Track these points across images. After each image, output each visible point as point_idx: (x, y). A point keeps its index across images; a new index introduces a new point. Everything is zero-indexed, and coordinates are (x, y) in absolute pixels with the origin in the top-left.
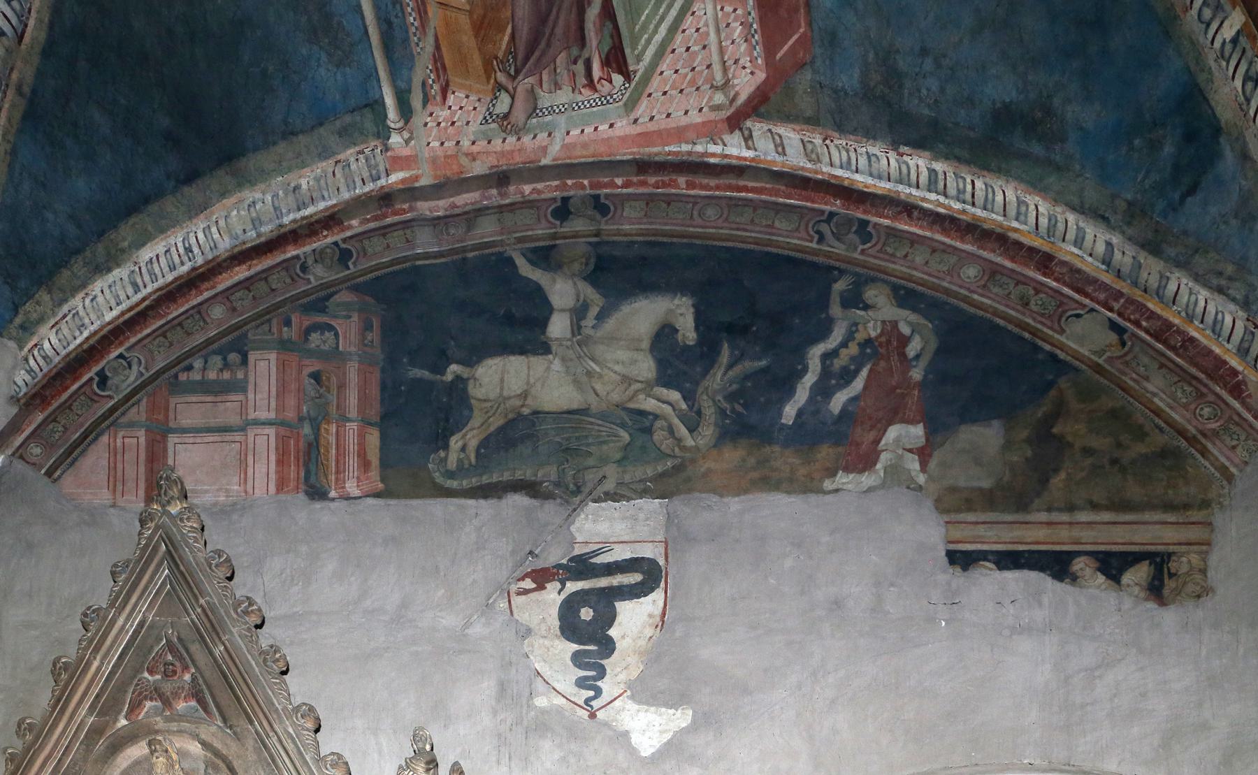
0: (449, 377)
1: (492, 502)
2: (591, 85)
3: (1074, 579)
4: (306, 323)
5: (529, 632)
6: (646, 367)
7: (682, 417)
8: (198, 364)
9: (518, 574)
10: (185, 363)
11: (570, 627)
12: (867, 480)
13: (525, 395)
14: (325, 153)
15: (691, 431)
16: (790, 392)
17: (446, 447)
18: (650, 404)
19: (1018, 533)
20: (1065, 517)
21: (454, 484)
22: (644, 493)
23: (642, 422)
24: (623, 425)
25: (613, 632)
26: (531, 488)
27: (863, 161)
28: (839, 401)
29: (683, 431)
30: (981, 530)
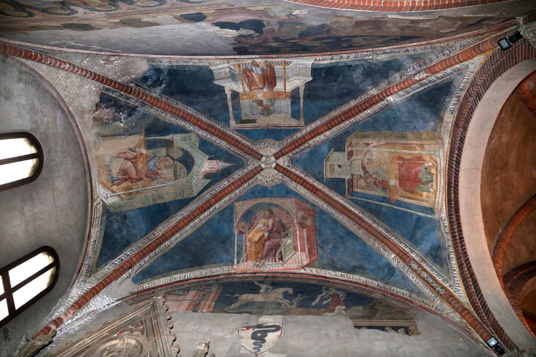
0: (235, 296)
1: (239, 315)
2: (275, 262)
3: (386, 331)
4: (205, 287)
5: (242, 337)
6: (281, 296)
7: (289, 304)
8: (177, 291)
9: (243, 327)
10: (175, 291)
11: (254, 337)
12: (332, 314)
13: (252, 299)
14: (220, 267)
15: (291, 305)
16: (314, 301)
17: (231, 306)
18: (281, 302)
19: (370, 323)
20: (381, 321)
21: (231, 311)
22: (278, 314)
23: (279, 304)
24: (274, 304)
25: (266, 338)
26: (250, 313)
27: (328, 273)
28: (325, 302)
29: (289, 306)
30: (362, 322)
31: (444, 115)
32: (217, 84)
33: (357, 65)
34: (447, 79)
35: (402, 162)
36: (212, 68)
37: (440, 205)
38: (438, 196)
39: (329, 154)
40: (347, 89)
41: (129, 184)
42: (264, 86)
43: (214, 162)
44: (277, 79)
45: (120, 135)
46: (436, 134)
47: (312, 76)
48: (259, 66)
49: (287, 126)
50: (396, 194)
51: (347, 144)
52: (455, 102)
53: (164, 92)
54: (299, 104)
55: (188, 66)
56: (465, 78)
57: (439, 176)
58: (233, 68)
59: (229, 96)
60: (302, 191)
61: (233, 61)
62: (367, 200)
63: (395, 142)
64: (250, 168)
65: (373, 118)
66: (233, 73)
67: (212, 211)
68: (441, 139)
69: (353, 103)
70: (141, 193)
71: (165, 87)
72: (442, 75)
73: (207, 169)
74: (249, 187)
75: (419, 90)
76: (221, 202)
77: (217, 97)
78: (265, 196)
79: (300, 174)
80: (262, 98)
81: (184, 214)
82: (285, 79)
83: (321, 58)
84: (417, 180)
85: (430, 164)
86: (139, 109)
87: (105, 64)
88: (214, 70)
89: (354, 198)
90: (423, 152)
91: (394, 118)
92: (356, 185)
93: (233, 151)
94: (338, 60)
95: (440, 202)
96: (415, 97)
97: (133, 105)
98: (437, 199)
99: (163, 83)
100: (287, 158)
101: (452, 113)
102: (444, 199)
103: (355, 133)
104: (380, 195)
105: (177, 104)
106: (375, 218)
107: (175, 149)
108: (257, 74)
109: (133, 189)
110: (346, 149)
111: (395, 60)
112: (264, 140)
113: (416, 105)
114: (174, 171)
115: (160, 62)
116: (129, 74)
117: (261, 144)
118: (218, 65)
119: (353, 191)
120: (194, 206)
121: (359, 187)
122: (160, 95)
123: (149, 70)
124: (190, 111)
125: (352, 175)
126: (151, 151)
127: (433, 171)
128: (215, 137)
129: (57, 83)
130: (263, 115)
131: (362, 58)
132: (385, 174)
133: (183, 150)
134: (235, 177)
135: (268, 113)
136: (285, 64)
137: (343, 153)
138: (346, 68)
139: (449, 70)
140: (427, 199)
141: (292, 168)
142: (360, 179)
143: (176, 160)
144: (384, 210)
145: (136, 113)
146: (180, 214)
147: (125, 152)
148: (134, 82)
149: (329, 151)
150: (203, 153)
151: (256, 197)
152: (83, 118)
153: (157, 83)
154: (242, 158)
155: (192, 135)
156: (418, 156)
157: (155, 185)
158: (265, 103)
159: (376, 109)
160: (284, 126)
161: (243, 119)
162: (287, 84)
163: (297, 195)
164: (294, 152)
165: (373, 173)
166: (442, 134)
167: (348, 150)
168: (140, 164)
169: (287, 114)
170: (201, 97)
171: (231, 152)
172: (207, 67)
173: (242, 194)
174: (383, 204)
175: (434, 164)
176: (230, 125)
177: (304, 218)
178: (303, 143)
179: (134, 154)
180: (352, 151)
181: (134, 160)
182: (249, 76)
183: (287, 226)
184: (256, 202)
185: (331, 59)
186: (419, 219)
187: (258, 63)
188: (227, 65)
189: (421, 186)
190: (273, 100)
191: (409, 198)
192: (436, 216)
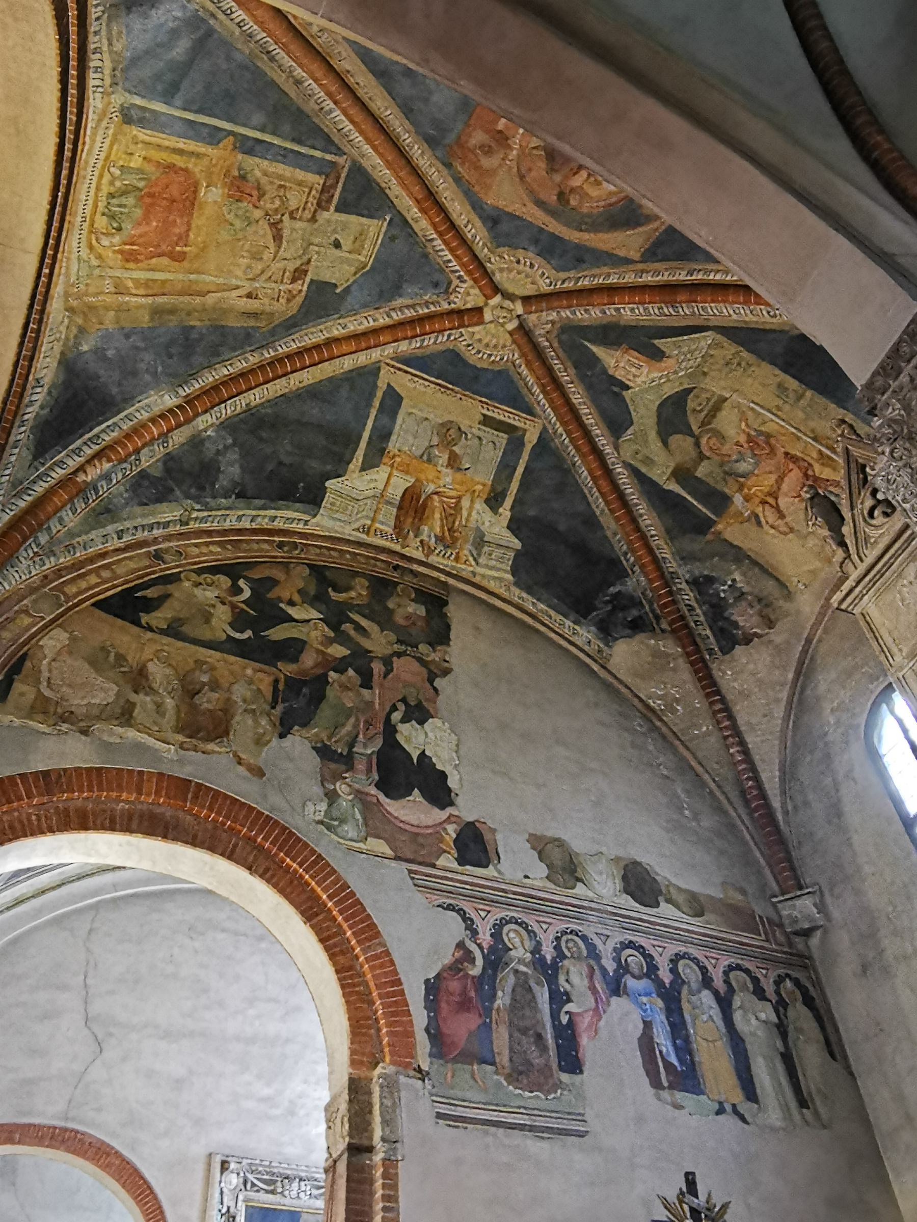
31: (56, 375)
32: (516, 541)
33: (226, 498)
34: (43, 464)
35: (178, 248)
36: (509, 577)
37: (101, 132)
38: (103, 155)
39: (351, 281)
40: (261, 439)
41: (817, 468)
42: (429, 497)
43: (619, 375)
44: (397, 503)
45: (755, 563)
46: (80, 321)
47: (326, 488)
48: (422, 542)
49: (421, 381)
50: (214, 162)
51: (299, 299)
52: (29, 410)
53: (623, 574)
54: (374, 428)
55: (549, 606)
56: (7, 477)
57: (89, 209)
58: (471, 559)
59: (508, 502)
60: (459, 210)
61: (464, 574)
62: (296, 148)
63: (181, 299)
64: (553, 315)
65: (219, 355)
66: (476, 549)
67: (701, 273)
68: (70, 309)
69: (255, 397)
70: (813, 431)
71: (613, 585)
72: (54, 475)
73: (645, 370)
74: (580, 275)
75: (104, 426)
76: (665, 278)
77: (532, 513)
78: (556, 239)
79: (442, 250)
80: (444, 470)
81: (765, 313)
82: (381, 497)
83: (294, 525)
84: (148, 200)
85: (105, 242)
86: (687, 576)
87: (677, 701)
88: (505, 571)
89: (328, 157)
90: (118, 273)
91: (170, 356)
92: (314, 192)
93: (565, 371)
94: (262, 513)
95: (99, 139)
96: (116, 409)
97: (692, 591)
98: (106, 146)
99: (612, 595)
100: (456, 300)
101: (38, 381)
102: (87, 147)
103: (272, 325)
104: (257, 160)
105: (615, 534)
106: (292, 91)
107: (679, 458)
108: (431, 529)
109: (820, 450)
110: (305, 288)
111: (146, 504)
112: (485, 366)
113: (115, 390)
114: (714, 416)
115: (589, 642)
116: (656, 654)
117: (498, 359)
118: (494, 578)
119: (327, 176)
120: (731, 312)
121: (306, 187)
122: (634, 573)
123: (617, 639)
124: (599, 505)
125: (313, 219)
126: (727, 490)
127: (101, 222)
128: (586, 422)
129: (771, 733)
130: (459, 429)
131: (214, 513)
132: (230, 217)
133: (665, 443)
134: (598, 313)
135: (448, 430)
136: (369, 528)
137: (315, 278)
138: (249, 493)
139: (40, 488)
140: (132, 148)
141: (457, 271)
142: (298, 209)
143: (691, 434)
144: (258, 118)
145: (697, 573)
146: (774, 320)
147: (772, 527)
148: (658, 630)
149: (348, 287)
150: (631, 408)
151: (579, 247)
152: (788, 642)
153: (623, 602)
154: (556, 345)
155: (627, 452)
156: (131, 265)
157: (773, 424)
158: (444, 458)
159: (207, 375)
160: (427, 383)
161: (506, 436)
162: (382, 487)
163: (477, 206)
164: (433, 308)
165: (257, 221)
166: (66, 321)
167: (302, 285)
168: (766, 483)
169: (410, 410)
170: (562, 527)
171: (572, 371)
172: (516, 584)
173: (606, 270)
174: (258, 135)
175: (97, 240)
176: (541, 433)
177: (488, 151)
178: (401, 324)
179: (760, 510)
180: (294, 280)
181: (771, 500)
182: (449, 530)
183: (543, 153)
184: (586, 236)
185: (273, 519)
186: (168, 96)
187: (420, 549)
188: (479, 570)
189: (141, 184)
190: (425, 458)
191: (180, 152)
192: (119, 99)
